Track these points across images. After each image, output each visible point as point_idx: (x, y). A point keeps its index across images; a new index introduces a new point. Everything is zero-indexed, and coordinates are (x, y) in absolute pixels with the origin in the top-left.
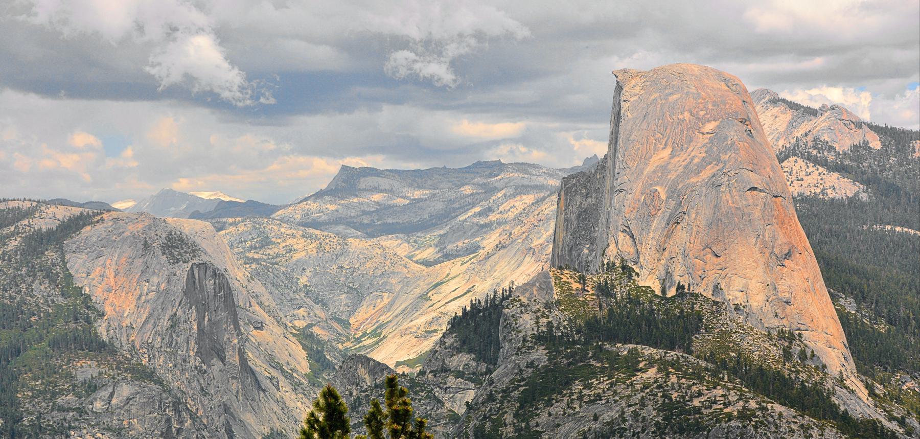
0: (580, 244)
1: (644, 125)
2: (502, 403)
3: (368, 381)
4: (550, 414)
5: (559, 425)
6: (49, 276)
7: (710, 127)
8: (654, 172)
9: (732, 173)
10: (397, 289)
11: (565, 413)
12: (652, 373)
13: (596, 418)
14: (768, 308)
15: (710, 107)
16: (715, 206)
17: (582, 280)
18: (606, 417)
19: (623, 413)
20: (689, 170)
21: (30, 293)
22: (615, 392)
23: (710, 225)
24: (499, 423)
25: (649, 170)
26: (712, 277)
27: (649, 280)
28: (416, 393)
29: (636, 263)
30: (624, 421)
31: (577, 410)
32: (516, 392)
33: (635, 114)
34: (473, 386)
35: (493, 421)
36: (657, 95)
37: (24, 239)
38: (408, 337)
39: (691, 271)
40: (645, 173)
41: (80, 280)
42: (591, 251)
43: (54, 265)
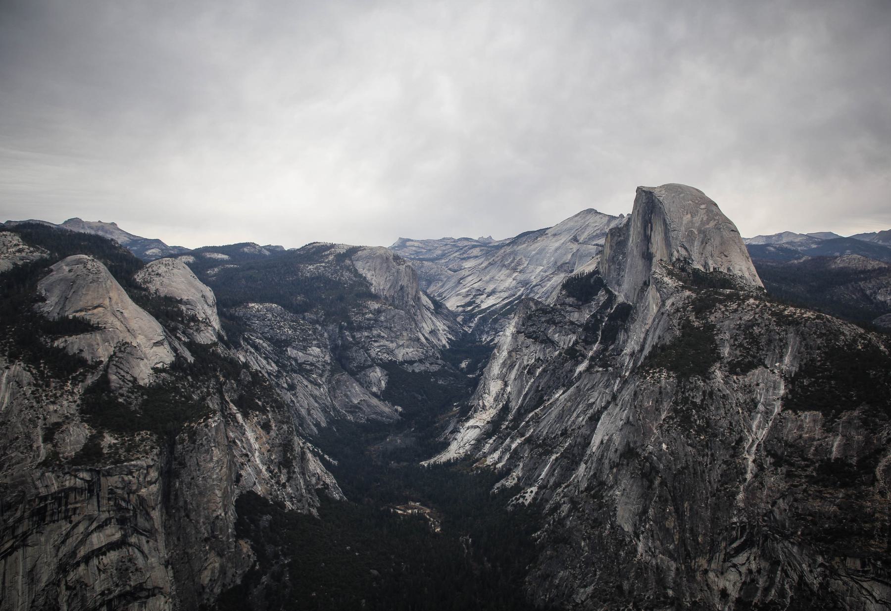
3: (534, 308)
4: (716, 317)
6: (348, 269)
7: (703, 206)
10: (445, 280)
12: (752, 301)
13: (741, 319)
14: (751, 278)
18: (746, 318)
21: (342, 275)
22: (743, 309)
23: (721, 244)
24: (688, 321)
26: (726, 265)
27: (698, 266)
28: (555, 313)
30: (757, 320)
34: (577, 310)
37: (335, 256)
38: (459, 296)
40: (684, 223)
41: (361, 271)
43: (350, 266)
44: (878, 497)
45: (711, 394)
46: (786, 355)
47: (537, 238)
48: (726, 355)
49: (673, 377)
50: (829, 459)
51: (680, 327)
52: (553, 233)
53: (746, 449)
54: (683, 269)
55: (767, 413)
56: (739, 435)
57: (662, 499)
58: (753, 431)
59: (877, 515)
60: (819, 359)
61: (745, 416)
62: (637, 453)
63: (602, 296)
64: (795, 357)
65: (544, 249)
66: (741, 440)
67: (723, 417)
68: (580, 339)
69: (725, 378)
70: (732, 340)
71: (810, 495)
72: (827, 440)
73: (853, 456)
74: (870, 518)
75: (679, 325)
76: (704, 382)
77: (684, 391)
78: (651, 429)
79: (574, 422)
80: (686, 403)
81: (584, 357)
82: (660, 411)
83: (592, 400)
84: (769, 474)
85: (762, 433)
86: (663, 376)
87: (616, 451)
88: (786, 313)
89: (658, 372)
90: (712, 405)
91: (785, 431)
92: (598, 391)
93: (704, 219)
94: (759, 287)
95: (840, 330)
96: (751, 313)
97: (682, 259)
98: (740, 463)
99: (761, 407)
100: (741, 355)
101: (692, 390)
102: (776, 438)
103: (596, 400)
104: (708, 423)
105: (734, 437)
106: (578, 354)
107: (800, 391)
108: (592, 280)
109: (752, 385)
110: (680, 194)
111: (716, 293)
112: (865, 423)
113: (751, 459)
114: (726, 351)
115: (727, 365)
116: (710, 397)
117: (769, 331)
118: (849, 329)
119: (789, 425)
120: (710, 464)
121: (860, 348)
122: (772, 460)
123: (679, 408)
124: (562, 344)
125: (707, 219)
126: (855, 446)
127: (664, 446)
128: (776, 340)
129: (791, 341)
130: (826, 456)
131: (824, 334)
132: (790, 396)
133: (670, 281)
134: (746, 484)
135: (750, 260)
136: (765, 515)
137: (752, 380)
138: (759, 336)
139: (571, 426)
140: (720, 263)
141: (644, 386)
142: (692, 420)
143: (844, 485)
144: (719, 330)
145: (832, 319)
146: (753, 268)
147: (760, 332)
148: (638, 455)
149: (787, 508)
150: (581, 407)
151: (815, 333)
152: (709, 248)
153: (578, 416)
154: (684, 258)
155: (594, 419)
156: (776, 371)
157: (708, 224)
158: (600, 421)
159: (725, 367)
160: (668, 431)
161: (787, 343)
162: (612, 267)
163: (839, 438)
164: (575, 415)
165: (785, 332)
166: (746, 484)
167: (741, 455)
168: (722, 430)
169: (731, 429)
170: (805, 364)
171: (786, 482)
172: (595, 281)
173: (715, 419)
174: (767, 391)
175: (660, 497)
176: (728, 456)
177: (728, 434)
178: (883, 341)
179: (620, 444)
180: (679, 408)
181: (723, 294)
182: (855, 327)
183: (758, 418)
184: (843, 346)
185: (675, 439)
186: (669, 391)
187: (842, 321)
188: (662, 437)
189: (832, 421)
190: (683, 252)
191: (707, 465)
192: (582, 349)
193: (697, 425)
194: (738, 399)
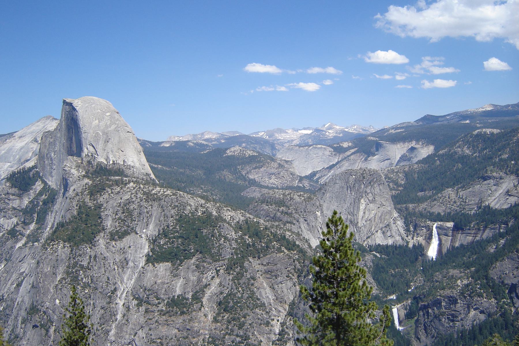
0: (50, 153)
1: (87, 113)
2: (82, 196)
4: (104, 198)
5: (109, 202)
7: (108, 114)
8: (95, 127)
9: (121, 127)
11: (109, 198)
12: (132, 184)
13: (121, 199)
15: (106, 108)
16: (119, 137)
17: (82, 160)
19: (131, 196)
20: (107, 126)
22: (124, 191)
23: (119, 143)
24: (84, 202)
25: (92, 127)
27: (101, 159)
29: (96, 154)
30: (133, 199)
31: (113, 196)
32: (86, 192)
33: (82, 110)
34: (19, 198)
35: (82, 202)
36: (87, 105)
39: (115, 156)
42: (55, 155)
44: (203, 319)
45: (95, 257)
46: (150, 224)
47: (6, 140)
48: (109, 227)
49: (68, 247)
50: (174, 296)
51: (78, 208)
52: (19, 135)
53: (119, 296)
54: (89, 162)
55: (136, 267)
56: (114, 287)
57: (56, 342)
58: (124, 282)
59: (201, 331)
60: (172, 224)
61: (119, 272)
62: (38, 309)
63: (38, 186)
64: (156, 225)
65: (11, 149)
66: (115, 290)
67: (103, 274)
68: (20, 221)
69: (107, 244)
70: (114, 215)
71: (160, 324)
72: (173, 282)
73: (189, 292)
74: (197, 334)
75: (77, 206)
76: (91, 248)
77: (75, 257)
78: (49, 289)
79: (9, 289)
80: (76, 266)
81: (22, 235)
82: (56, 275)
83: (22, 271)
84: (134, 313)
85: (130, 282)
86: (60, 247)
87: (26, 310)
88: (153, 192)
89: (57, 244)
90: (95, 266)
91: (146, 280)
92: (27, 262)
93: (108, 124)
94: (146, 174)
95: (188, 203)
96: (129, 193)
97: (90, 154)
98: (113, 307)
99: (131, 264)
100: (119, 226)
101: (80, 256)
102: (139, 286)
103: (26, 269)
104: (92, 280)
105: (110, 289)
106: (18, 233)
107: (157, 249)
108: (31, 174)
109: (126, 248)
110: (92, 105)
111: (108, 180)
112: (197, 267)
113: (121, 303)
114: (109, 223)
115: (109, 234)
116: (94, 259)
117: (140, 206)
118: (193, 200)
119: (149, 274)
120: (92, 311)
121: (200, 214)
122: (136, 302)
123: (70, 270)
124: (6, 226)
125: (110, 123)
126: (191, 284)
127: (57, 301)
128: (144, 212)
129: (155, 214)
130: (172, 294)
131: (177, 206)
132: (151, 254)
133: (76, 172)
134: (117, 322)
135: (142, 153)
136: (129, 343)
137: (126, 244)
138: (133, 210)
139: (7, 292)
140: (118, 157)
141: (45, 256)
142: (80, 279)
143: (183, 313)
144: (105, 208)
145: (184, 195)
146: (144, 159)
147: (134, 207)
148: (38, 311)
149: (145, 336)
150: (14, 276)
151: (170, 206)
152: (110, 145)
153: (12, 284)
154: (92, 153)
155: (19, 285)
156: (143, 236)
157: (111, 127)
158: (22, 287)
159: (107, 236)
160: (61, 289)
161: (152, 215)
162: (46, 162)
163: (182, 279)
164: (10, 283)
165: (151, 206)
166: (117, 322)
167: (115, 301)
168: (101, 284)
169: (108, 282)
170: (163, 229)
171: (144, 317)
172: (33, 175)
173: (97, 276)
174: (136, 251)
175: (54, 342)
176: (105, 304)
177: (106, 287)
178: (216, 208)
179: (28, 303)
180: (70, 270)
181: (113, 181)
182: (199, 199)
183: (128, 272)
184: (189, 213)
185: (65, 295)
186: (64, 258)
187: (190, 196)
188: (57, 295)
189: (177, 269)
190: (91, 149)
191: (89, 312)
192: (22, 229)
193: (83, 282)
194: (114, 259)
